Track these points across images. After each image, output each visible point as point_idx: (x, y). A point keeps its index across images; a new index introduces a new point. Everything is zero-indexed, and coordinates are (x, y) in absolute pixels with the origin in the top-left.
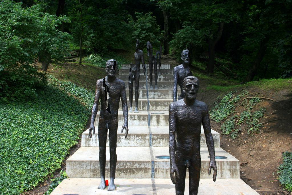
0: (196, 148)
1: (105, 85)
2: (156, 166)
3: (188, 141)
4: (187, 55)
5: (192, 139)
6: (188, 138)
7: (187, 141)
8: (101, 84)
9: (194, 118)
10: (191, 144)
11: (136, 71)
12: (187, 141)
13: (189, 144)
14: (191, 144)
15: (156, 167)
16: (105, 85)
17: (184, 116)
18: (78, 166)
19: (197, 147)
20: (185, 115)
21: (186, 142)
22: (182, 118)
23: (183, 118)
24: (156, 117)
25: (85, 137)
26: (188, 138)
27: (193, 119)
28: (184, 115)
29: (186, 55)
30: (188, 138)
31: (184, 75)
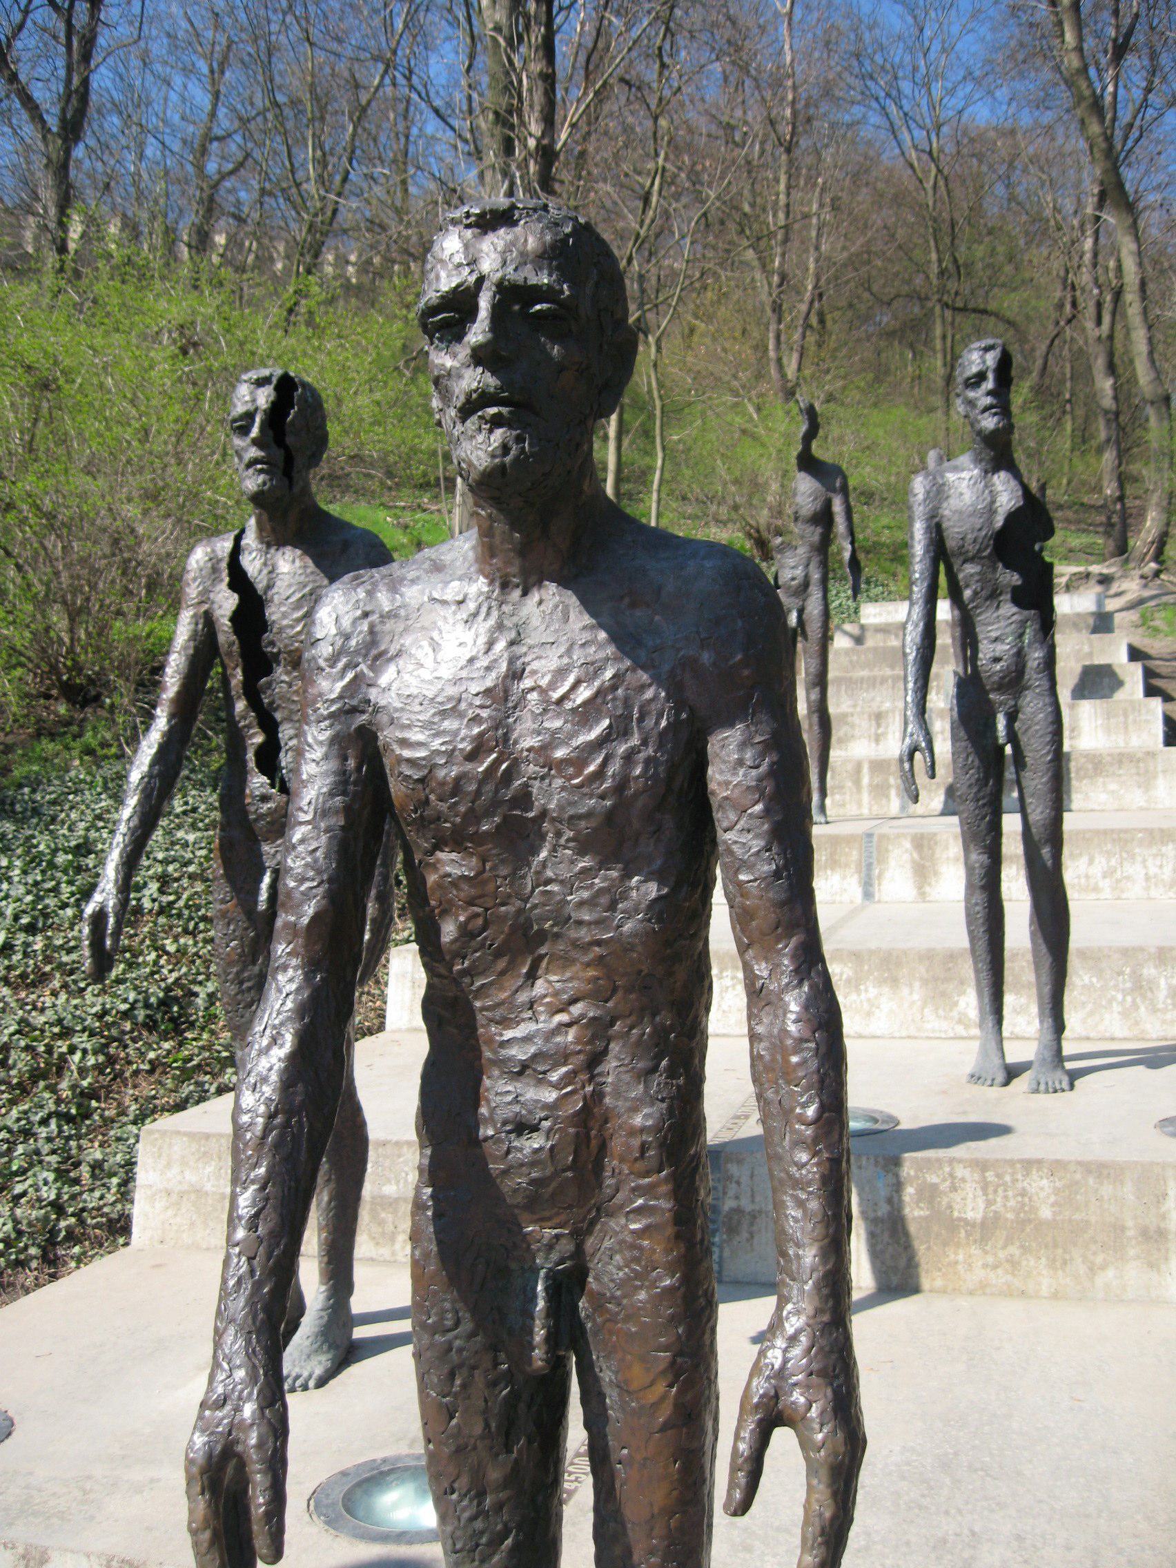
0: (633, 1132)
1: (239, 580)
2: (732, 1189)
3: (527, 1039)
4: (991, 376)
5: (577, 1009)
6: (531, 1005)
7: (508, 1034)
8: (215, 570)
9: (565, 743)
10: (554, 1077)
11: (806, 584)
12: (508, 1034)
13: (541, 1081)
14: (568, 1079)
15: (737, 1198)
16: (239, 580)
17: (447, 724)
18: (209, 1169)
19: (638, 1120)
20: (452, 710)
21: (504, 1052)
22: (420, 744)
23: (436, 744)
24: (908, 845)
25: (410, 968)
26: (523, 997)
27: (560, 753)
28: (443, 714)
29: (981, 377)
30: (523, 997)
31: (978, 522)
